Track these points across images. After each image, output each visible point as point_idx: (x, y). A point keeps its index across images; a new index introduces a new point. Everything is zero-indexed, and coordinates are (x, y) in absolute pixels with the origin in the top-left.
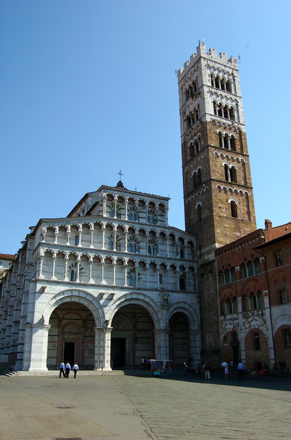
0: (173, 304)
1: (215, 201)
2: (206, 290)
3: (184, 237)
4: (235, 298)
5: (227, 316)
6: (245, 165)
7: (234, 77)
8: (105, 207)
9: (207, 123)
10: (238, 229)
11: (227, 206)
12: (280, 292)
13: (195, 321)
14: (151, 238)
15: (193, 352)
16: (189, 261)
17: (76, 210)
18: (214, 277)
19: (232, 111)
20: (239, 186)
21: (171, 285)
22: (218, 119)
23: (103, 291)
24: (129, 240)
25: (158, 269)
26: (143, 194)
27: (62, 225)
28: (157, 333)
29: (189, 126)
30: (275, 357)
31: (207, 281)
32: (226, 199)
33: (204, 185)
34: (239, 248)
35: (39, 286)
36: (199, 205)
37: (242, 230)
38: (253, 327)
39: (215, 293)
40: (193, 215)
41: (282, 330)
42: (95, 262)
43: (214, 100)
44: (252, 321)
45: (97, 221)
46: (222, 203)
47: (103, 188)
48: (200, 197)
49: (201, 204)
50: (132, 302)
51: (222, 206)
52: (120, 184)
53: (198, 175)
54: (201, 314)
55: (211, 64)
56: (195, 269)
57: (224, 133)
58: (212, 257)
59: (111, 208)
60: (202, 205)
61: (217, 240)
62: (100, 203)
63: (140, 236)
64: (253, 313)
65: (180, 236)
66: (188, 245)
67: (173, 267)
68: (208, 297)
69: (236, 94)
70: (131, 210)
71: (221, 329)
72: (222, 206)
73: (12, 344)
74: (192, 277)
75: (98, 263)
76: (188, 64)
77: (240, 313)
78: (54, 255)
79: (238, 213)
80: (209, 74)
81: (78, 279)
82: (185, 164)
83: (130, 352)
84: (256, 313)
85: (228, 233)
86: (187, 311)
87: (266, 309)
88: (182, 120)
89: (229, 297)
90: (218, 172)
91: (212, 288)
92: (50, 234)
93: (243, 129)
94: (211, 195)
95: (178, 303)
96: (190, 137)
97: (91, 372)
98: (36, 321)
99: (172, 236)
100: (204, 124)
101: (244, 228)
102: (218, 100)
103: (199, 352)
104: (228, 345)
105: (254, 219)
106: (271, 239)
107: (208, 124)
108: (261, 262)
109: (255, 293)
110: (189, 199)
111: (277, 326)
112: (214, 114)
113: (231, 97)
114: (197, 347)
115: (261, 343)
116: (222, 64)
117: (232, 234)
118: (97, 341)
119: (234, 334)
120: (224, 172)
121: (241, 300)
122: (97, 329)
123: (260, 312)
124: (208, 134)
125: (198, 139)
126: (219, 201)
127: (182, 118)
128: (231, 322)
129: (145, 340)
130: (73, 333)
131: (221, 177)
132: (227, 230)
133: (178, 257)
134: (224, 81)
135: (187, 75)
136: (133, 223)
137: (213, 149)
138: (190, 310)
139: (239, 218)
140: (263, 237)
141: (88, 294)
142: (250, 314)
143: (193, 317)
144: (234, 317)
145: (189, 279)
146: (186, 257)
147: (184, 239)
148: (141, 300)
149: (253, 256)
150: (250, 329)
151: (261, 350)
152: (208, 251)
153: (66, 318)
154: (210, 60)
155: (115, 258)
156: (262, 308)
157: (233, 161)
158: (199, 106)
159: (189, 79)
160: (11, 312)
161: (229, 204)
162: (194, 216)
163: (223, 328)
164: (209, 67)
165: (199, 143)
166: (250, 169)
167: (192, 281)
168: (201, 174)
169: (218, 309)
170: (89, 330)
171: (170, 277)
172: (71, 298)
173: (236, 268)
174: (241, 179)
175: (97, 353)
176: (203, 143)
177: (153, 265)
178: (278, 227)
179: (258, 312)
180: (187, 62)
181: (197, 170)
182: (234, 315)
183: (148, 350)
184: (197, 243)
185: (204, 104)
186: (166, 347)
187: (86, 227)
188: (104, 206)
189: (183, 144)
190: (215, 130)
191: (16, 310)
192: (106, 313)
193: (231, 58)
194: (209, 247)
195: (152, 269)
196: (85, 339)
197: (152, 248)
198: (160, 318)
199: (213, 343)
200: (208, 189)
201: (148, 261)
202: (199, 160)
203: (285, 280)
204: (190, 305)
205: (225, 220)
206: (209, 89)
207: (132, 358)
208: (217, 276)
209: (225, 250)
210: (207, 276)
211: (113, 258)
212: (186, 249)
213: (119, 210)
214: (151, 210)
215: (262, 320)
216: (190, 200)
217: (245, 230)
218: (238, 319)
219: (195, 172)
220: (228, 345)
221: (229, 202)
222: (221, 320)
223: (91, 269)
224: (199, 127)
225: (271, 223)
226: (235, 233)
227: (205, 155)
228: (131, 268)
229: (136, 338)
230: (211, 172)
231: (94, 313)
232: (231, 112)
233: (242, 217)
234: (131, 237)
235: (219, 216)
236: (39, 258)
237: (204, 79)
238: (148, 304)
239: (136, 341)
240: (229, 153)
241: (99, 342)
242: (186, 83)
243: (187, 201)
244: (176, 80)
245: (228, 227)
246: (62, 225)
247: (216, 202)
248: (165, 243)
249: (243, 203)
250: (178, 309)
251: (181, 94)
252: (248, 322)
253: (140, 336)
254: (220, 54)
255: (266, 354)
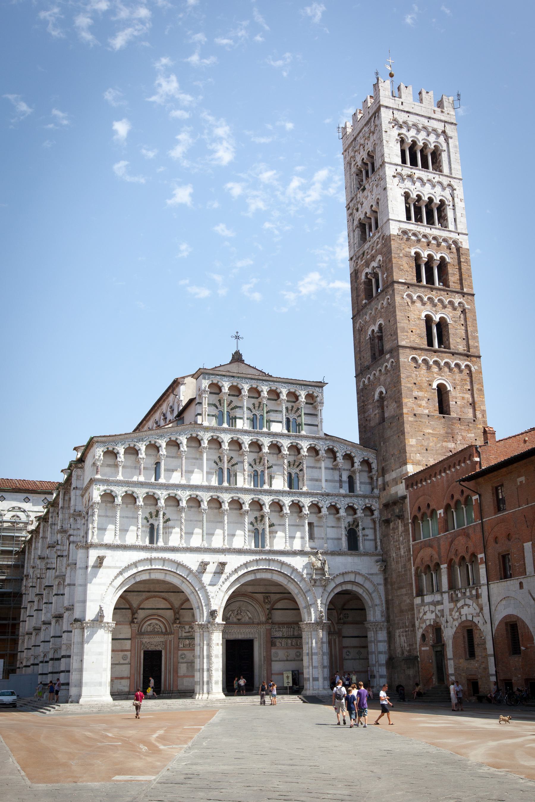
0: (334, 577)
1: (405, 387)
2: (394, 549)
3: (353, 453)
4: (438, 565)
5: (425, 597)
6: (466, 313)
7: (448, 139)
8: (205, 408)
9: (392, 238)
10: (451, 436)
11: (429, 393)
12: (504, 558)
13: (376, 605)
14: (293, 457)
15: (374, 663)
16: (365, 497)
17: (160, 406)
18: (406, 525)
19: (443, 208)
20: (453, 354)
21: (330, 541)
22: (412, 227)
23: (206, 557)
24: (253, 464)
25: (305, 514)
26: (275, 379)
27: (129, 445)
28: (306, 630)
29: (363, 238)
30: (496, 671)
31: (395, 533)
32: (428, 381)
33: (388, 356)
34: (442, 476)
35: (93, 554)
36: (381, 393)
37: (460, 438)
38: (464, 618)
39: (408, 555)
40: (371, 410)
41: (506, 624)
42: (192, 507)
43: (407, 190)
44: (462, 607)
45: (191, 434)
46: (420, 389)
47: (202, 373)
48: (382, 378)
49: (384, 392)
50: (259, 576)
51: (420, 394)
52: (237, 358)
53: (378, 336)
54: (387, 594)
55: (401, 117)
56: (375, 510)
57: (424, 255)
58: (401, 489)
59: (217, 408)
60: (386, 392)
61: (410, 459)
62: (197, 401)
63: (271, 455)
64: (464, 593)
65: (345, 452)
66: (360, 467)
67: (334, 509)
68: (397, 562)
69: (451, 174)
70: (254, 408)
71: (417, 620)
72: (420, 394)
73: (50, 656)
74: (371, 526)
75: (196, 509)
76: (359, 116)
77: (445, 592)
78: (118, 500)
79: (451, 406)
80: (397, 140)
81: (161, 540)
82: (357, 314)
83: (263, 663)
84: (468, 594)
85: (431, 444)
86: (361, 588)
87: (482, 587)
88: (351, 227)
89: (428, 563)
90: (412, 332)
91: (402, 547)
92: (110, 461)
93: (463, 243)
94: (399, 377)
95: (343, 574)
96: (364, 261)
97: (188, 701)
98: (90, 615)
99: (332, 452)
100: (387, 240)
101: (463, 434)
102: (415, 190)
103: (384, 662)
104: (428, 648)
105: (483, 415)
106: (493, 463)
107: (393, 239)
108: (474, 503)
109: (467, 558)
110: (364, 379)
111: (498, 617)
112: (405, 220)
113: (440, 180)
114: (380, 653)
115: (476, 646)
116: (422, 116)
117: (439, 445)
118: (199, 647)
119: (437, 630)
120: (425, 330)
121: (446, 570)
122: (197, 626)
123: (474, 592)
124: (393, 259)
125: (377, 267)
126: (414, 386)
127: (351, 223)
128: (432, 608)
129: (289, 641)
130: (158, 633)
131: (418, 340)
132: (429, 439)
133: (344, 491)
134: (428, 150)
135: (358, 139)
136: (258, 433)
137: (403, 288)
138: (367, 587)
139: (453, 415)
140: (477, 459)
141: (179, 565)
142: (459, 595)
143: (372, 599)
144: (436, 600)
145: (363, 529)
146: (358, 489)
147: (354, 457)
148: (275, 572)
149: (462, 492)
150: (459, 621)
151: (476, 659)
152: (395, 478)
153: (145, 607)
154: (398, 110)
155: (225, 499)
156: (477, 584)
157: (444, 307)
158: (378, 203)
159: (362, 147)
160: (48, 598)
161: (434, 389)
162: (374, 413)
163: (421, 619)
164: (395, 123)
165: (380, 275)
166: (476, 320)
167: (370, 533)
168: (384, 334)
169: (412, 584)
170: (187, 627)
171: (328, 527)
172: (150, 573)
173: (439, 512)
174: (459, 340)
175: (198, 668)
176: (385, 276)
177: (297, 507)
178: (510, 438)
179: (470, 591)
180: (358, 111)
181: (377, 326)
182: (436, 596)
183: (294, 660)
184: (378, 466)
185: (385, 200)
186: (321, 653)
187: (174, 446)
188: (204, 406)
189: (353, 275)
190: (407, 250)
191: (56, 595)
192: (213, 598)
193: (442, 98)
194: (397, 471)
195: (296, 515)
196: (180, 644)
197: (293, 475)
198: (310, 603)
199: (406, 645)
200: (394, 364)
201: (287, 501)
202: (379, 308)
203: (509, 537)
204: (367, 577)
205: (426, 420)
206: (396, 170)
207: (265, 675)
208: (410, 525)
209: (421, 480)
210: (395, 524)
211: (222, 499)
212: (358, 474)
213: (232, 409)
214: (293, 407)
215: (478, 605)
216: (366, 382)
217: (464, 438)
218: (442, 604)
219: (373, 330)
220: (428, 648)
221: (435, 386)
222: (417, 605)
223: (183, 521)
224: (380, 245)
225: (494, 433)
226: (445, 444)
227: (388, 299)
228: (257, 514)
229: (272, 638)
230: (398, 332)
231: (191, 598)
232: (442, 209)
233: (460, 413)
234: (256, 457)
235: (415, 415)
236: (92, 506)
237: (386, 150)
238: (288, 577)
239: (273, 644)
240: (434, 293)
241: (202, 649)
242: (356, 153)
243: (361, 384)
244: (339, 146)
245: (431, 433)
246: (129, 445)
247: (408, 388)
248: (318, 465)
249: (462, 386)
250: (344, 586)
251: (348, 176)
252: (458, 609)
253: (279, 634)
254: (420, 93)
255: (484, 666)
